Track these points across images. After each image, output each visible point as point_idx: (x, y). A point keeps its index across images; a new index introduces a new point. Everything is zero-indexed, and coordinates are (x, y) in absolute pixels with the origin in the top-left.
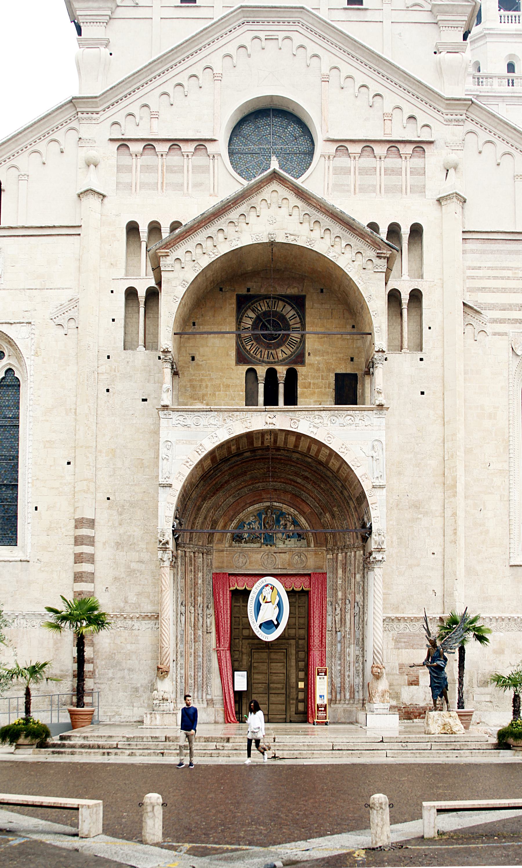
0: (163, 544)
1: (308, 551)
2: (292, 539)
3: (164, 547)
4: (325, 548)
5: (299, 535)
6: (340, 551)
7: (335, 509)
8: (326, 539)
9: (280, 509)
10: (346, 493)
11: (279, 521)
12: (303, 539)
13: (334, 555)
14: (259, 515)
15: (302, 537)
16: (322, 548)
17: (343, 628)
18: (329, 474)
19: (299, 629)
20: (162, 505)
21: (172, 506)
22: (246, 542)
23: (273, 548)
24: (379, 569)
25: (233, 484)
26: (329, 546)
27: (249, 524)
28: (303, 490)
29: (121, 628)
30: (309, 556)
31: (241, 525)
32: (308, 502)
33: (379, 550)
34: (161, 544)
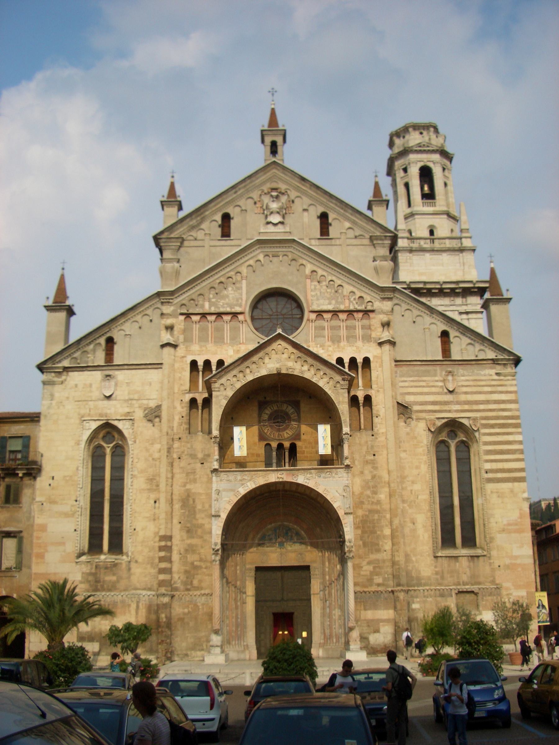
0: (216, 551)
27: (269, 536)
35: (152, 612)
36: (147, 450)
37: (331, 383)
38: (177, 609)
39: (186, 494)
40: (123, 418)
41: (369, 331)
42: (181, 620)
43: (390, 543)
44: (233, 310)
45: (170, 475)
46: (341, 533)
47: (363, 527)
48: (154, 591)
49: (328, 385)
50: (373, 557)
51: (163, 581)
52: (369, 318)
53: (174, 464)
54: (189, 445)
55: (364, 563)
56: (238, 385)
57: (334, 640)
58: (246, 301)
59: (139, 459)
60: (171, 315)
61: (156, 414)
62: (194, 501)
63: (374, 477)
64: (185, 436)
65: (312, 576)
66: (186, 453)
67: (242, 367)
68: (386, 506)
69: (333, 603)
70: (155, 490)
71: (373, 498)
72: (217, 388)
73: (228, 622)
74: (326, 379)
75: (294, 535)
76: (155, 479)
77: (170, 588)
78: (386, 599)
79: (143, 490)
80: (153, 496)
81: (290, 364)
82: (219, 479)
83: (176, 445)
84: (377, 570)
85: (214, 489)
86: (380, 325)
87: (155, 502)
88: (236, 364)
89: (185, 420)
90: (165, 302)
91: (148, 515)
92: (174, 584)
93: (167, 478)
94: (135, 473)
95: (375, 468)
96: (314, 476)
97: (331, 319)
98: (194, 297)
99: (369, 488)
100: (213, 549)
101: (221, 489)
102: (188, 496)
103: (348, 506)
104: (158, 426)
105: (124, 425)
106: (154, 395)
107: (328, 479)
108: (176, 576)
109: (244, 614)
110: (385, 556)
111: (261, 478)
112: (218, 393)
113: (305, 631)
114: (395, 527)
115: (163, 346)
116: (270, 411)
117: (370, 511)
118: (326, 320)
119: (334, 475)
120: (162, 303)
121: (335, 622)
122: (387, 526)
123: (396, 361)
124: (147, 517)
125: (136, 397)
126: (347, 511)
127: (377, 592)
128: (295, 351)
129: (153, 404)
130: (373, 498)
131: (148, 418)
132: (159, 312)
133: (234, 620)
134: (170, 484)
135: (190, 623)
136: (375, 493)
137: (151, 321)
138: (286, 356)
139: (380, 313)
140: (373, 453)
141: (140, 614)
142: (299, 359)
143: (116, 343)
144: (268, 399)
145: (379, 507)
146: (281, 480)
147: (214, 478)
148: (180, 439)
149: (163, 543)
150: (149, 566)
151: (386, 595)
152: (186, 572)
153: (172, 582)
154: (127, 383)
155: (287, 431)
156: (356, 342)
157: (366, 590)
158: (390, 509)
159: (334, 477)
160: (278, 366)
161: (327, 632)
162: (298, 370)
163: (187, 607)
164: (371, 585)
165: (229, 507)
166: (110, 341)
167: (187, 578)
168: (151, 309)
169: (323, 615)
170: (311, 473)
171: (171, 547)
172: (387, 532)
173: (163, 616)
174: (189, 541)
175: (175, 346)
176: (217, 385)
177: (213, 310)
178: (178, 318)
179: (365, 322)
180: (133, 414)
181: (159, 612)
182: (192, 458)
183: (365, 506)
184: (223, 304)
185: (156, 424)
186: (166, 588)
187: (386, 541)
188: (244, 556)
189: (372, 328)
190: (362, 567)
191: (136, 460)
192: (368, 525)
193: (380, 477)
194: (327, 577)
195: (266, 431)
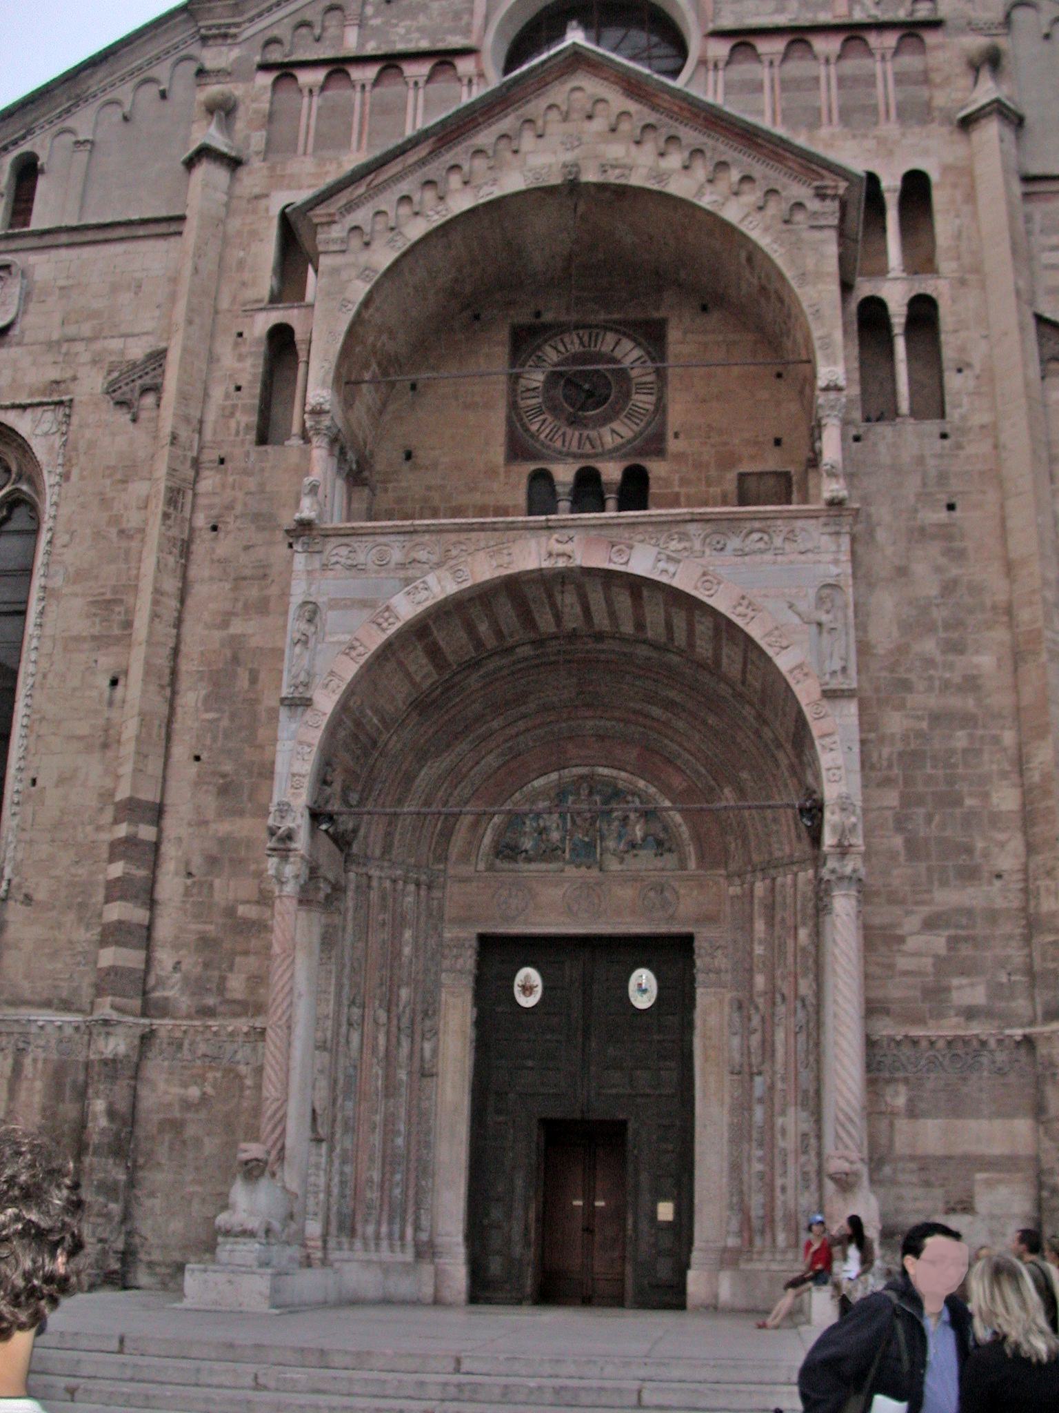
2: (642, 853)
3: (282, 846)
4: (723, 872)
5: (660, 843)
6: (759, 875)
7: (745, 775)
8: (726, 851)
9: (611, 783)
10: (767, 733)
12: (670, 850)
15: (667, 845)
18: (723, 689)
22: (529, 860)
25: (495, 724)
26: (733, 867)
28: (666, 737)
30: (682, 891)
31: (515, 820)
32: (679, 762)
34: (274, 839)
35: (68, 1093)
36: (105, 502)
37: (773, 208)
38: (162, 1086)
39: (228, 653)
40: (37, 400)
41: (924, 92)
42: (176, 1126)
43: (1016, 843)
44: (440, 46)
45: (171, 585)
46: (810, 779)
47: (908, 780)
48: (79, 1011)
49: (759, 216)
50: (948, 897)
51: (113, 970)
52: (922, 48)
53: (194, 547)
54: (252, 483)
55: (912, 923)
56: (416, 230)
57: (781, 1238)
58: (487, 18)
59: (72, 534)
60: (229, 74)
61: (147, 380)
62: (254, 679)
63: (949, 588)
64: (242, 447)
65: (700, 977)
66: (239, 508)
67: (433, 170)
68: (1001, 700)
69: (779, 1085)
70: (118, 640)
71: (950, 666)
72: (334, 241)
73: (348, 1144)
74: (751, 197)
76: (119, 602)
77: (136, 1003)
78: (1000, 1072)
79: (78, 639)
80: (107, 662)
81: (616, 151)
82: (316, 562)
83: (208, 482)
84: (965, 950)
85: (296, 599)
86: (960, 67)
87: (114, 682)
88: (412, 158)
89: (252, 396)
90: (215, 37)
91: (83, 728)
92: (154, 989)
93: (157, 591)
94: (57, 582)
95: (958, 555)
96: (697, 545)
97: (786, 57)
98: (308, 15)
99: (931, 628)
101: (321, 600)
102: (235, 660)
103: (837, 665)
104: (151, 420)
105: (37, 422)
106: (148, 321)
107: (758, 558)
108: (165, 958)
109: (421, 1119)
110: (1001, 895)
111: (481, 555)
112: (338, 260)
113: (665, 1198)
114: (1036, 777)
115: (190, 164)
117: (936, 718)
118: (766, 59)
119: (778, 541)
120: (204, 39)
121: (784, 1163)
122: (1004, 775)
123: (1027, 179)
124: (81, 738)
125: (86, 329)
126: (834, 684)
127: (965, 1041)
128: (632, 106)
129: (137, 350)
130: (950, 666)
131: (117, 395)
132: (192, 67)
133: (377, 1139)
134: (169, 614)
135: (206, 1140)
136: (956, 648)
137: (163, 95)
138: (599, 125)
139: (961, 31)
140: (944, 499)
141: (23, 1095)
142: (650, 135)
143: (42, 171)
144: (548, 317)
145: (970, 703)
146: (561, 563)
147: (300, 561)
148: (222, 461)
149: (122, 830)
150: (71, 917)
151: (1001, 1057)
153: (152, 981)
154: (62, 288)
155: (616, 425)
156: (876, 124)
157: (916, 1032)
158: (1018, 710)
160: (569, 157)
161: (756, 1202)
162: (643, 171)
163: (200, 1079)
164: (939, 1015)
165: (349, 670)
166: (27, 171)
167: (206, 965)
168: (168, 63)
169: (740, 1134)
170: (684, 537)
171: (156, 846)
172: (1006, 799)
173: (99, 1105)
174: (224, 828)
175: (234, 163)
176: (337, 231)
177: (371, 48)
178: (252, 79)
179: (910, 61)
180: (72, 386)
181: (90, 1091)
182: (261, 529)
183: (912, 700)
184: (408, 32)
185: (144, 415)
186: (118, 1000)
187: (1001, 837)
188: (436, 894)
189: (937, 78)
190: (901, 939)
191: (62, 539)
192: (929, 771)
193: (976, 589)
194: (760, 981)
195: (534, 428)
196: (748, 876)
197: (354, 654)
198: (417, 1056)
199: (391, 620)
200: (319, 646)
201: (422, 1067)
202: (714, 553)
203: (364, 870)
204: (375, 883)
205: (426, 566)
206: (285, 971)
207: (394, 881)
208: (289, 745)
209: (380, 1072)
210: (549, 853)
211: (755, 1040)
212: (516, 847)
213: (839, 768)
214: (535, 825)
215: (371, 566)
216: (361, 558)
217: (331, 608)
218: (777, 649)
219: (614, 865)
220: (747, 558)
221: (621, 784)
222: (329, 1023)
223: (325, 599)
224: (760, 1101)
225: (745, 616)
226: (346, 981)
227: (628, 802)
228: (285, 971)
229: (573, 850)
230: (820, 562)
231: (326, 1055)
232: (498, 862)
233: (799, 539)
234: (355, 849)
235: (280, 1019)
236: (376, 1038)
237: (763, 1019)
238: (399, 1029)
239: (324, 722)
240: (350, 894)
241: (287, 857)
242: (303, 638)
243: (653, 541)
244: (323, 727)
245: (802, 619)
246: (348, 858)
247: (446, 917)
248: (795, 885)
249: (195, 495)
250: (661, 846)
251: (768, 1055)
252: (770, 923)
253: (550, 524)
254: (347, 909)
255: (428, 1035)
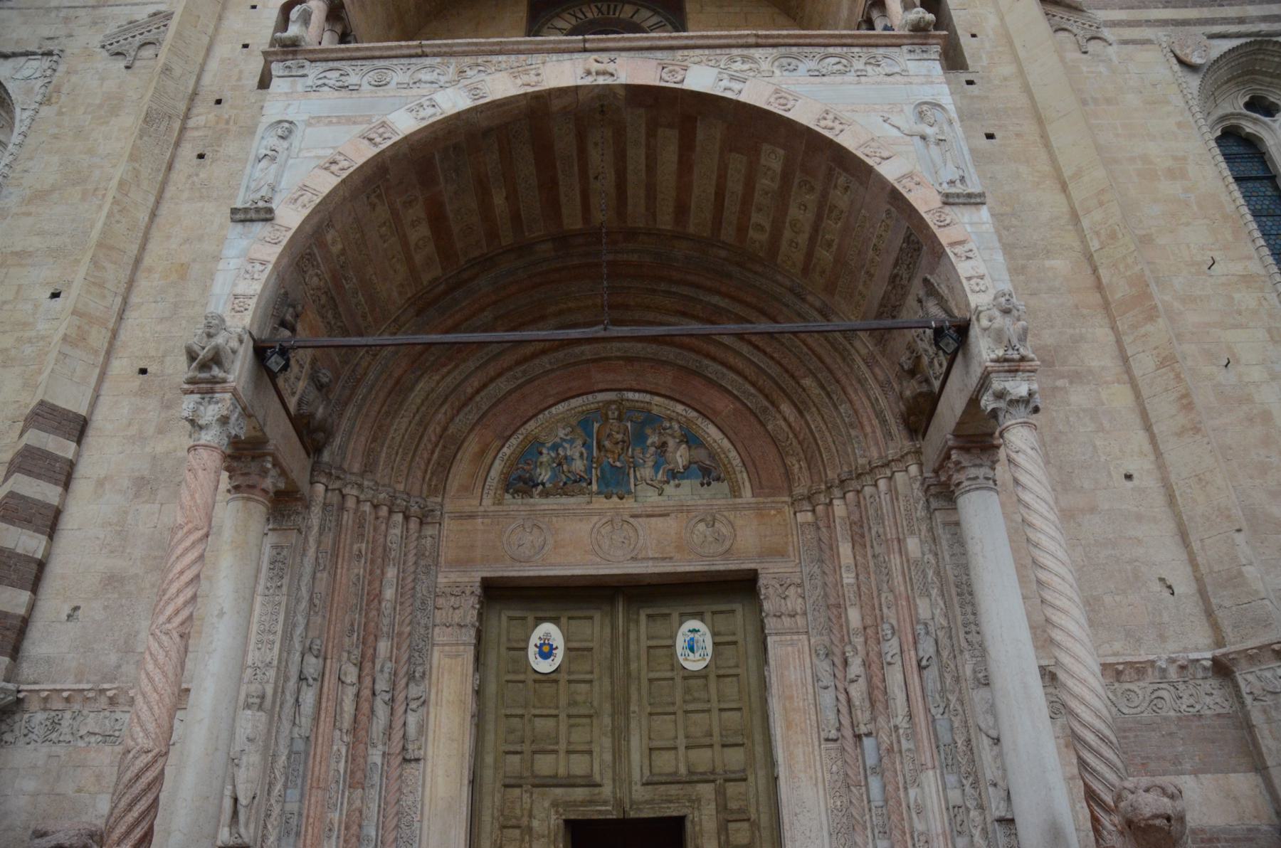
0: (204, 366)
1: (735, 508)
2: (686, 482)
6: (837, 492)
8: (788, 475)
11: (646, 437)
12: (718, 479)
13: (820, 508)
14: (585, 424)
15: (714, 474)
16: (777, 499)
17: (881, 720)
19: (724, 746)
20: (231, 262)
21: (262, 268)
22: (546, 494)
23: (629, 503)
24: (1024, 432)
26: (800, 490)
27: (555, 447)
29: (93, 739)
30: (739, 522)
31: (532, 448)
33: (1013, 366)
65: (771, 624)
75: (671, 443)
96: (765, 66)
100: (192, 356)
107: (839, 78)
116: (574, 22)
146: (601, 81)
152: (112, 581)
159: (860, 74)
165: (327, 183)
188: (429, 531)
194: (854, 616)
196: (822, 498)
197: (334, 168)
198: (397, 736)
199: (386, 136)
200: (291, 161)
201: (404, 748)
202: (786, 73)
203: (337, 484)
204: (351, 503)
205: (436, 85)
206: (187, 550)
207: (376, 507)
208: (234, 263)
209: (344, 751)
210: (570, 485)
211: (858, 691)
212: (531, 479)
213: (982, 277)
214: (553, 455)
215: (365, 87)
216: (353, 79)
217: (308, 124)
218: (878, 160)
219: (650, 498)
220: (825, 79)
221: (655, 410)
222: (272, 673)
223: (305, 117)
224: (878, 770)
225: (832, 129)
226: (301, 620)
227: (664, 429)
228: (187, 550)
229: (602, 479)
230: (911, 83)
231: (262, 716)
232: (508, 496)
233: (883, 63)
234: (326, 456)
235: (169, 620)
236: (339, 703)
237: (866, 664)
238: (374, 694)
239: (285, 238)
240: (316, 511)
241: (212, 392)
242: (270, 153)
243: (712, 63)
244: (284, 243)
245: (902, 132)
246: (315, 468)
247: (442, 559)
248: (892, 490)
249: (183, 129)
250: (708, 472)
251: (880, 706)
252: (858, 540)
253: (587, 45)
254: (309, 528)
255: (413, 705)
